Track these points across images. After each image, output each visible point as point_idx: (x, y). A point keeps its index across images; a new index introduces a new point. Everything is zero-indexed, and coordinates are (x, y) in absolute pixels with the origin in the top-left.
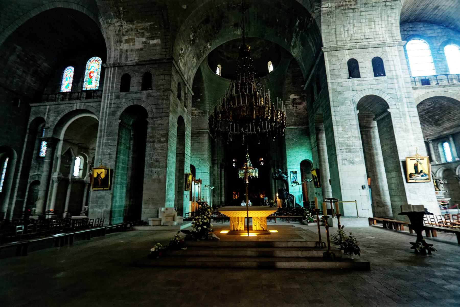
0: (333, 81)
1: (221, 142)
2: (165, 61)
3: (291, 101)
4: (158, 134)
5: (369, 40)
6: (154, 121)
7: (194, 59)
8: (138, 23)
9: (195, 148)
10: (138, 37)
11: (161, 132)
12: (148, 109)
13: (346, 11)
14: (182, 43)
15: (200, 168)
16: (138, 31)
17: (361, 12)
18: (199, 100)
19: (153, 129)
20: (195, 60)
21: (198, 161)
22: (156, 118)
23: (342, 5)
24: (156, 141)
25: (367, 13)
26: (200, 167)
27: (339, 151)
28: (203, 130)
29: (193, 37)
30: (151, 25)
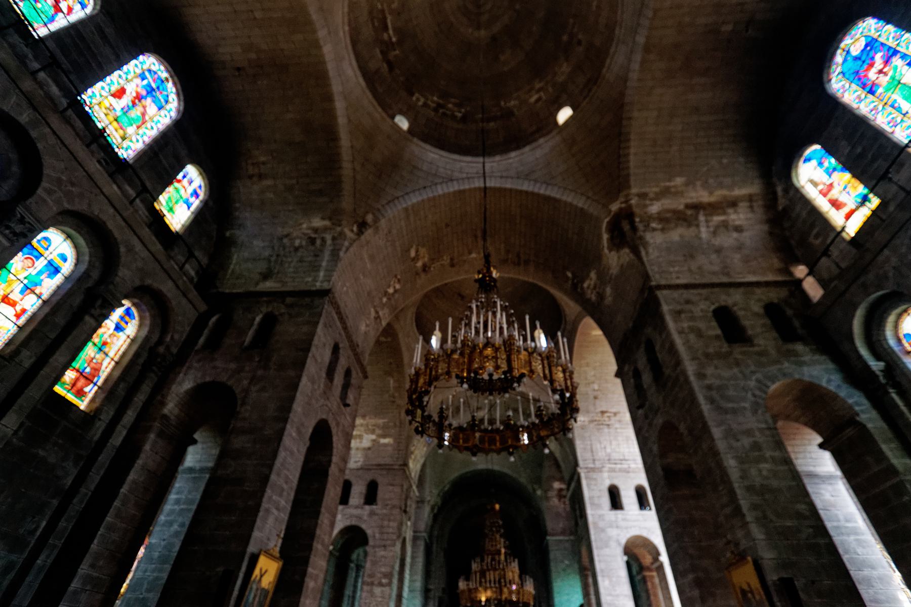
0: (593, 512)
1: (442, 554)
2: (397, 467)
3: (554, 493)
4: (381, 573)
5: (629, 462)
6: (375, 552)
8: (370, 418)
10: (367, 434)
11: (383, 570)
12: (369, 532)
13: (601, 427)
17: (616, 428)
19: (374, 563)
22: (379, 546)
23: (595, 421)
24: (376, 582)
25: (623, 431)
30: (384, 423)
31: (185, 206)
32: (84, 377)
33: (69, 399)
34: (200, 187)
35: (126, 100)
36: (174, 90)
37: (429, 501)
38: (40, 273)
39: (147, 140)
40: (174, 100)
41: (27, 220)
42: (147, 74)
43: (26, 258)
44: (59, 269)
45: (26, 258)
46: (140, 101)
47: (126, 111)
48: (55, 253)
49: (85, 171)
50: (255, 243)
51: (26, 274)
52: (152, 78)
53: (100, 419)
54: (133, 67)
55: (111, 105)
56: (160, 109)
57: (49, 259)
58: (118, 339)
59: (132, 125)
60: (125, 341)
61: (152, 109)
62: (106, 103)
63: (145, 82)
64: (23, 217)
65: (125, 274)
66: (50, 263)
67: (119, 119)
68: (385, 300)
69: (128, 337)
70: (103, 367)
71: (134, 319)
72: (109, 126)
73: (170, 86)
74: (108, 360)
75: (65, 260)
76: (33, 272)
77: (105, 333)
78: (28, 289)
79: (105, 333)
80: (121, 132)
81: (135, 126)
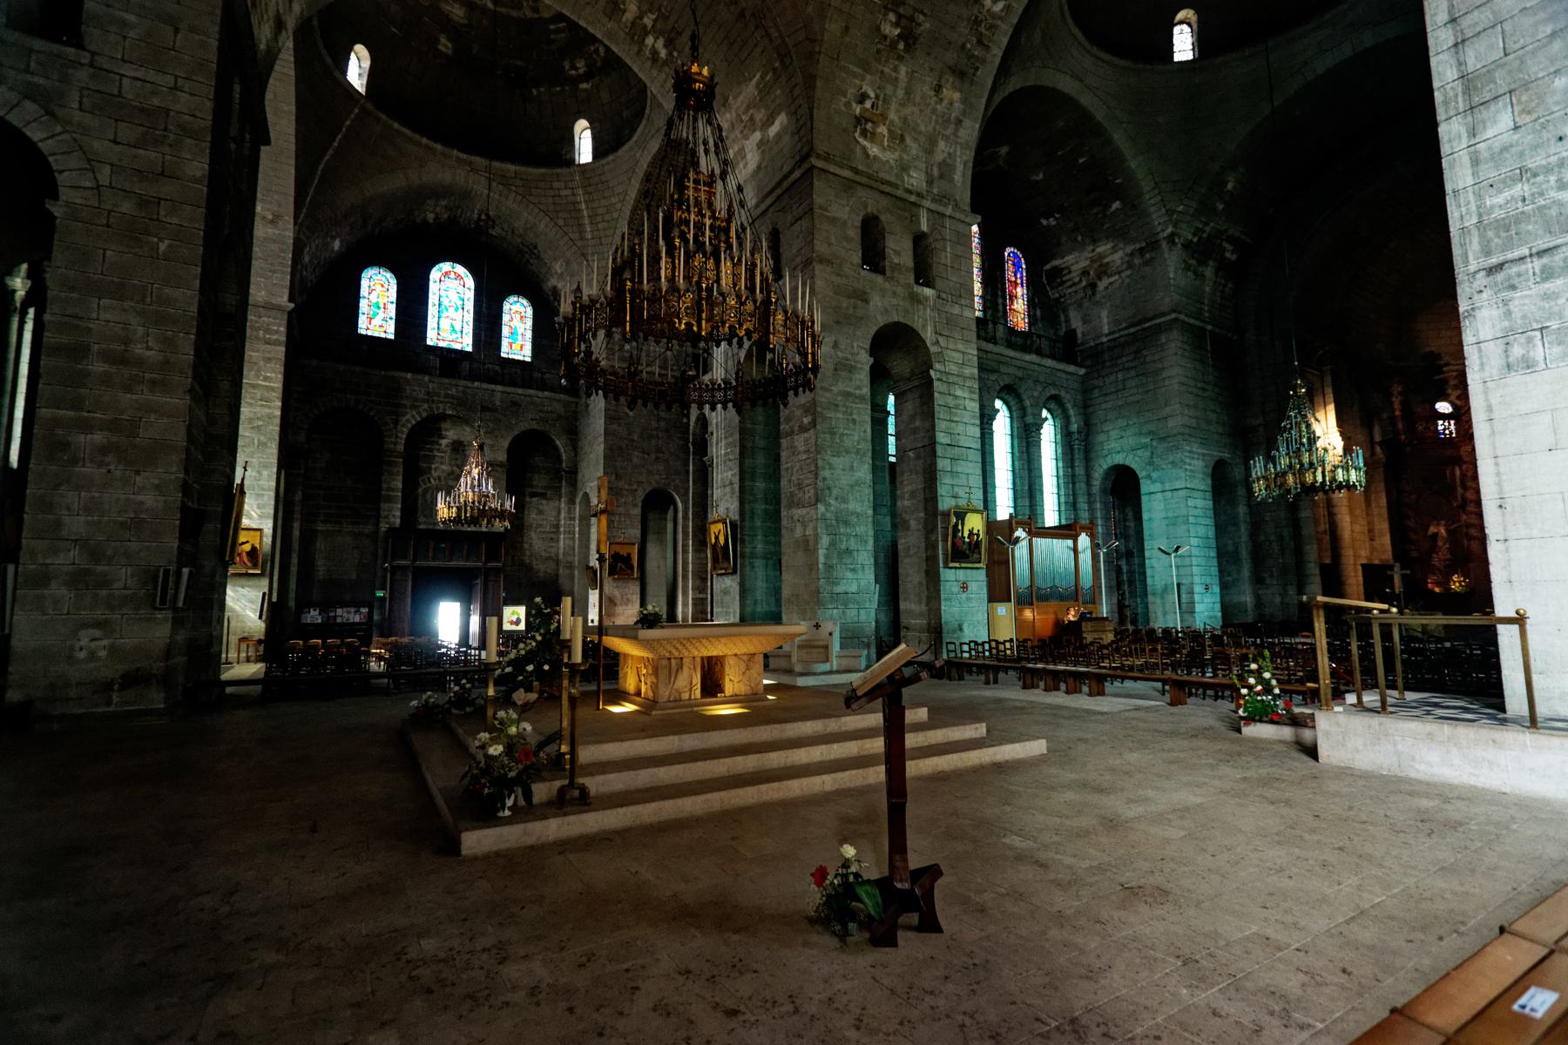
7: (947, 93)
8: (735, 98)
9: (1132, 399)
14: (855, 75)
15: (1155, 475)
16: (742, 121)
18: (1116, 205)
20: (952, 94)
21: (1145, 447)
26: (1156, 469)
27: (1481, 279)
28: (1154, 318)
29: (897, 25)
37: (1172, 235)
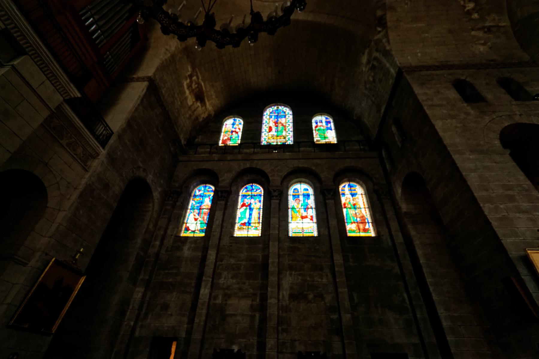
31: (329, 131)
32: (360, 223)
33: (363, 236)
34: (326, 118)
35: (274, 129)
36: (283, 107)
38: (304, 201)
39: (292, 130)
40: (286, 109)
41: (275, 189)
42: (271, 114)
43: (296, 200)
44: (309, 194)
45: (296, 200)
46: (277, 123)
47: (277, 131)
48: (302, 191)
49: (276, 159)
50: (363, 105)
51: (300, 205)
52: (273, 113)
53: (383, 235)
54: (266, 118)
55: (272, 135)
56: (285, 117)
57: (302, 194)
58: (358, 199)
59: (283, 132)
60: (362, 197)
61: (283, 120)
62: (270, 136)
63: (273, 117)
64: (273, 190)
65: (326, 175)
66: (304, 195)
67: (278, 135)
68: (476, 16)
69: (362, 194)
70: (365, 214)
71: (356, 186)
72: (278, 140)
73: (280, 108)
74: (363, 210)
75: (307, 190)
76: (302, 202)
77: (350, 201)
78: (306, 209)
79: (350, 201)
80: (282, 137)
81: (284, 131)
